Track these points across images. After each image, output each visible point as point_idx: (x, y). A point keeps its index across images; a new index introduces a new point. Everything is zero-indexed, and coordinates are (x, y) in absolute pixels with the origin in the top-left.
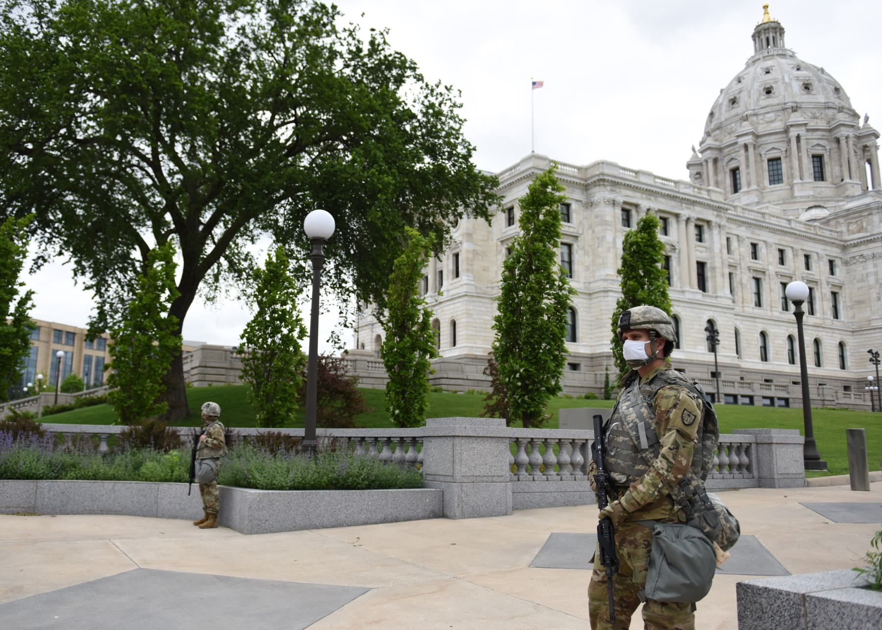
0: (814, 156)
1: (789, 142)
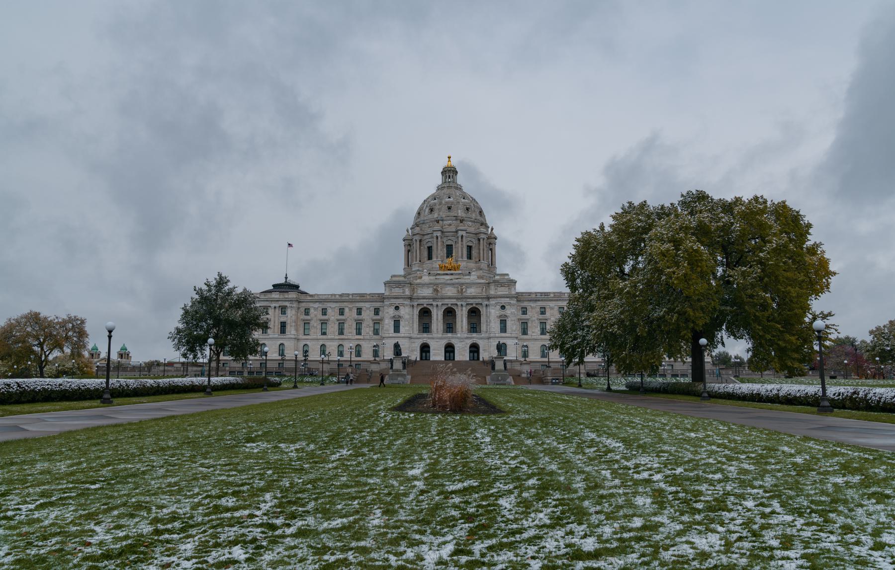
0: (468, 246)
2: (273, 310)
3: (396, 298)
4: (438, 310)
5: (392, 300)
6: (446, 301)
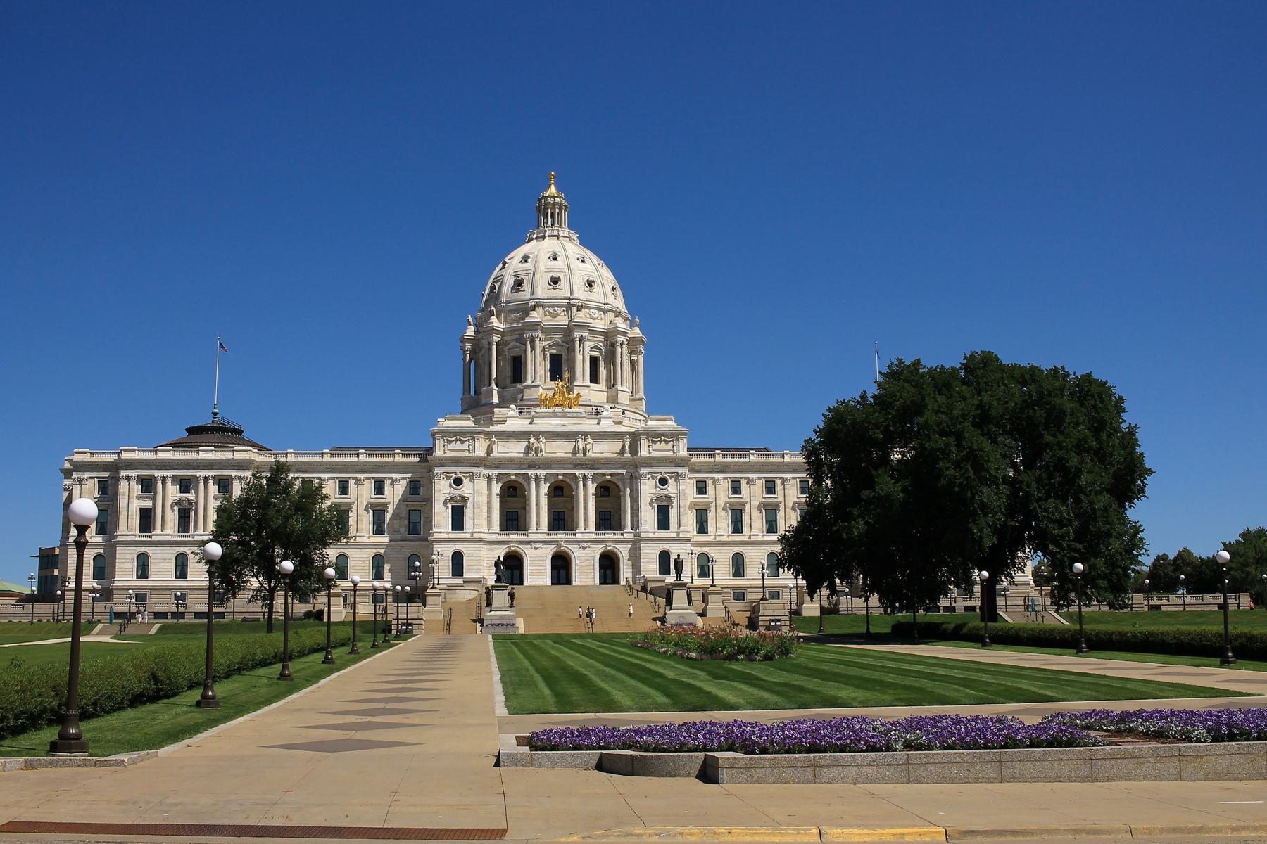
3: (457, 462)
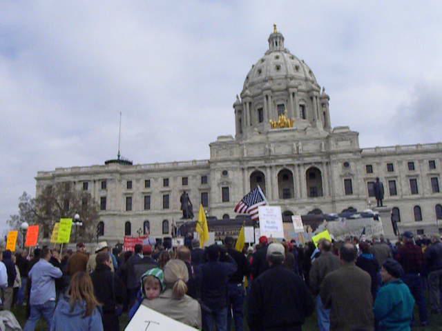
1: (289, 96)
2: (93, 184)
3: (225, 161)
4: (272, 173)
5: (219, 164)
6: (281, 161)
